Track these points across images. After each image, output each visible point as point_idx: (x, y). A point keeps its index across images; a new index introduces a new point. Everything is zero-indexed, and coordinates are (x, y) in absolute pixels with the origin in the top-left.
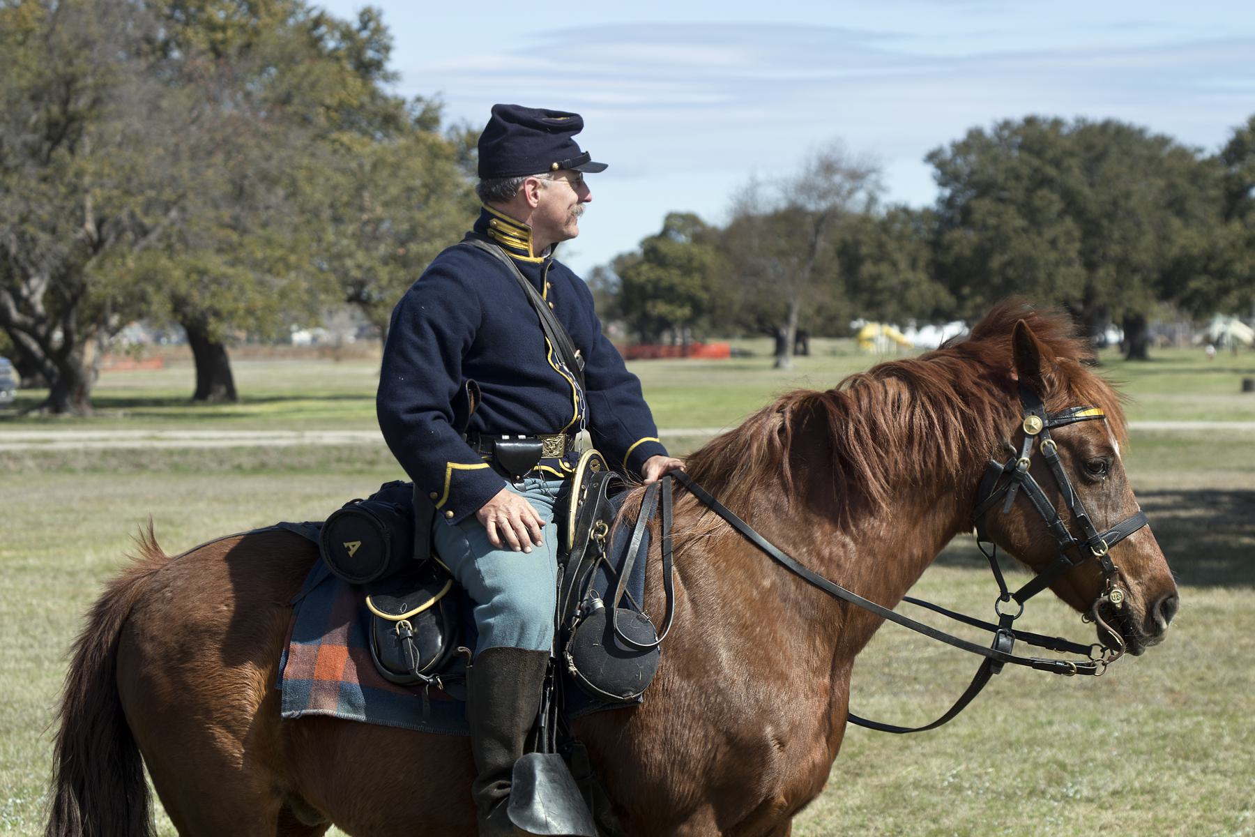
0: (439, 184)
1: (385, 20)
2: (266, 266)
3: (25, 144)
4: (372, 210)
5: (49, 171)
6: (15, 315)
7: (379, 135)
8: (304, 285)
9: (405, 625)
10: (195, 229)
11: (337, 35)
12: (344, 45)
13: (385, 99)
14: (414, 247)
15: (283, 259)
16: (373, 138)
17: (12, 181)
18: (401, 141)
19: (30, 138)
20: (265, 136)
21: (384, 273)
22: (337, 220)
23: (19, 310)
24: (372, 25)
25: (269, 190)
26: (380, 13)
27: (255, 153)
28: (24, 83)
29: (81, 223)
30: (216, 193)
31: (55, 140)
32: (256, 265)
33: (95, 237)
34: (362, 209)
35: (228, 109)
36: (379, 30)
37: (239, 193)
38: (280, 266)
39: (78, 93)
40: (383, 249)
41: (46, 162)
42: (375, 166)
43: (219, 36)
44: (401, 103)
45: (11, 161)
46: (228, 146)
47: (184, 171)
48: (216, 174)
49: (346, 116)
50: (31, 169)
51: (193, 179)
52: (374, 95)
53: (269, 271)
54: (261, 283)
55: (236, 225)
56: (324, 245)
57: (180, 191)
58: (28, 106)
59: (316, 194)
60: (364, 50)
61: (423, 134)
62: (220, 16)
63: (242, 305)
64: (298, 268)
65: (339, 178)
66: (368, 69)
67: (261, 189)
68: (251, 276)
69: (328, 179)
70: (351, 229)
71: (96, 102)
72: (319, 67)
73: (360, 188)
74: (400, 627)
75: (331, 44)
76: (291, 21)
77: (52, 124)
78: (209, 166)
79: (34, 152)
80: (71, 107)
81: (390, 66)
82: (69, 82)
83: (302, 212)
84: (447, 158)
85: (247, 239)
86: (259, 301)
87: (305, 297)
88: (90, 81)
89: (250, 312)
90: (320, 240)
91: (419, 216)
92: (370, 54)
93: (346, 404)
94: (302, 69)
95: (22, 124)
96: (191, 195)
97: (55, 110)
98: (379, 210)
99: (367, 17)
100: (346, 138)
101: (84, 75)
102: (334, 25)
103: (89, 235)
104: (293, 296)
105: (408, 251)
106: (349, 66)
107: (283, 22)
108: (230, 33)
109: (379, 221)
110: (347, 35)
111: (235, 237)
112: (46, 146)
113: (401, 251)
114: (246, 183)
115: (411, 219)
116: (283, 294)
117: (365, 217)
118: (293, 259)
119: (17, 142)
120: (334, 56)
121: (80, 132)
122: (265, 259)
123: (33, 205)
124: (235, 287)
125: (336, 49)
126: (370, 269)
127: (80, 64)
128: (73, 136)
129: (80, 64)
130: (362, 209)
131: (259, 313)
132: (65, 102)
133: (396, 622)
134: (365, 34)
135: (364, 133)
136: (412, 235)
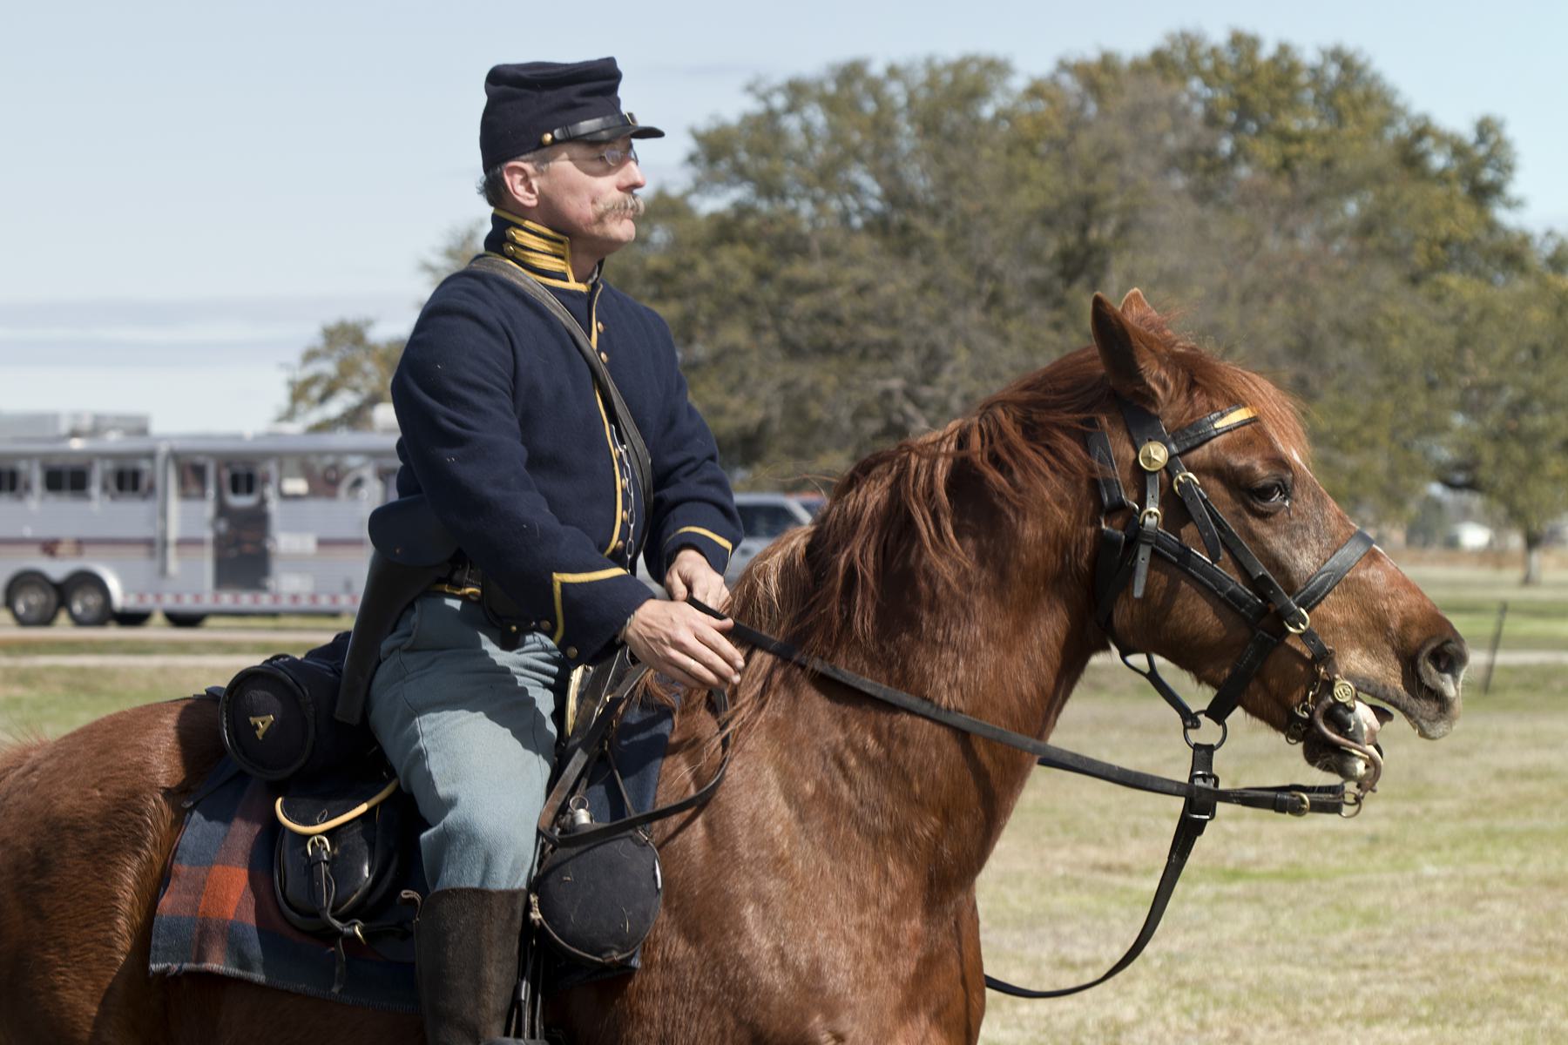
1: (1511, 132)
5: (1058, 315)
7: (1500, 278)
9: (321, 841)
11: (1448, 149)
12: (1455, 164)
13: (1507, 233)
15: (1354, 433)
16: (1490, 282)
17: (1013, 327)
18: (1522, 285)
19: (1039, 272)
20: (1342, 276)
21: (1488, 454)
24: (1492, 138)
26: (1501, 124)
27: (1326, 298)
28: (1032, 204)
30: (1275, 344)
31: (1070, 276)
34: (1463, 370)
35: (1306, 240)
36: (1501, 144)
39: (1103, 217)
40: (1490, 421)
41: (1059, 303)
42: (1482, 316)
43: (1294, 149)
44: (1526, 239)
45: (1013, 301)
46: (1297, 289)
47: (1230, 317)
48: (1274, 321)
49: (1452, 253)
50: (1039, 312)
52: (1492, 227)
58: (1036, 233)
59: (1402, 350)
60: (1480, 170)
61: (1551, 277)
62: (1295, 125)
66: (1483, 194)
69: (1420, 332)
71: (1123, 228)
72: (1411, 192)
74: (313, 844)
75: (1438, 161)
76: (1390, 134)
77: (1065, 256)
80: (1093, 234)
81: (1514, 189)
82: (1088, 206)
88: (1117, 201)
92: (1488, 175)
94: (1390, 190)
95: (1035, 256)
97: (1072, 239)
98: (1485, 374)
99: (1486, 128)
100: (1453, 280)
101: (1108, 195)
102: (1443, 139)
106: (1461, 190)
107: (1378, 134)
108: (1309, 146)
110: (1459, 150)
112: (1059, 284)
113: (1513, 425)
117: (1467, 381)
120: (1442, 177)
121: (1103, 266)
125: (1444, 170)
126: (1472, 448)
127: (1104, 183)
129: (1104, 183)
130: (1463, 370)
132: (1084, 229)
133: (308, 837)
134: (1482, 151)
135: (1477, 273)
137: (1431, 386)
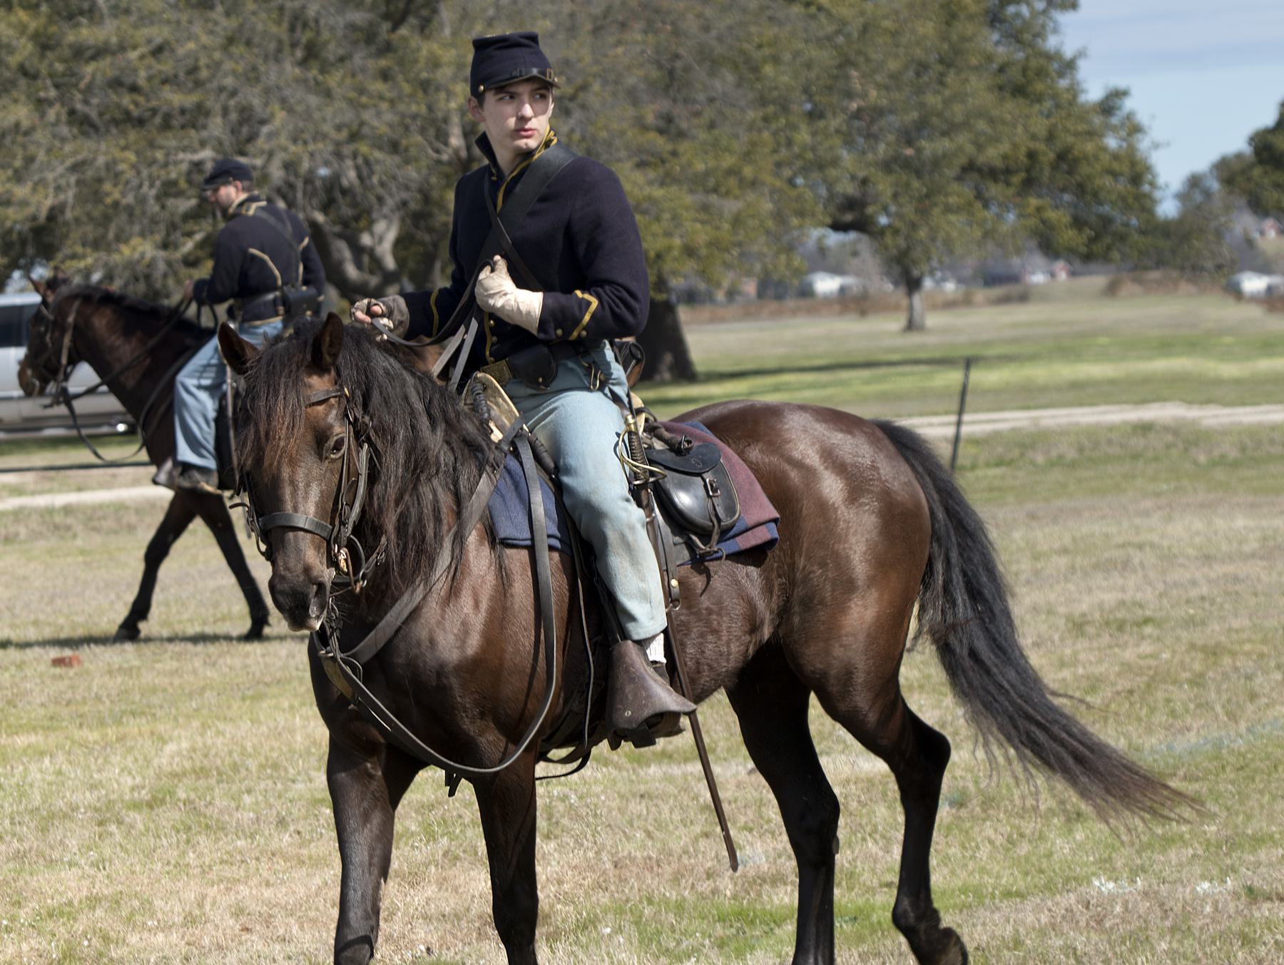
0: (957, 51)
2: (711, 182)
3: (352, 27)
4: (864, 95)
6: (352, 271)
8: (767, 206)
10: (604, 134)
14: (930, 147)
22: (815, 115)
23: (359, 265)
25: (712, 73)
29: (442, 136)
32: (697, 182)
33: (464, 154)
37: (671, 80)
38: (732, 182)
51: (597, 62)
53: (715, 190)
54: (705, 208)
55: (667, 126)
56: (796, 149)
57: (579, 81)
59: (778, 77)
63: (677, 242)
64: (754, 184)
65: (813, 52)
67: (700, 73)
68: (689, 199)
70: (835, 122)
73: (846, 63)
78: (619, 43)
79: (368, 36)
83: (763, 101)
84: (971, 17)
85: (684, 146)
86: (702, 236)
87: (770, 223)
89: (690, 251)
90: (790, 143)
91: (932, 100)
93: (844, 375)
96: (596, 87)
103: (456, 151)
104: (751, 222)
105: (919, 151)
109: (879, 112)
111: (661, 144)
114: (679, 64)
115: (922, 105)
116: (737, 221)
118: (748, 171)
119: (341, 21)
122: (707, 174)
123: (367, 115)
124: (667, 216)
128: (425, 13)
131: (704, 252)
136: (922, 125)
137: (815, 115)
